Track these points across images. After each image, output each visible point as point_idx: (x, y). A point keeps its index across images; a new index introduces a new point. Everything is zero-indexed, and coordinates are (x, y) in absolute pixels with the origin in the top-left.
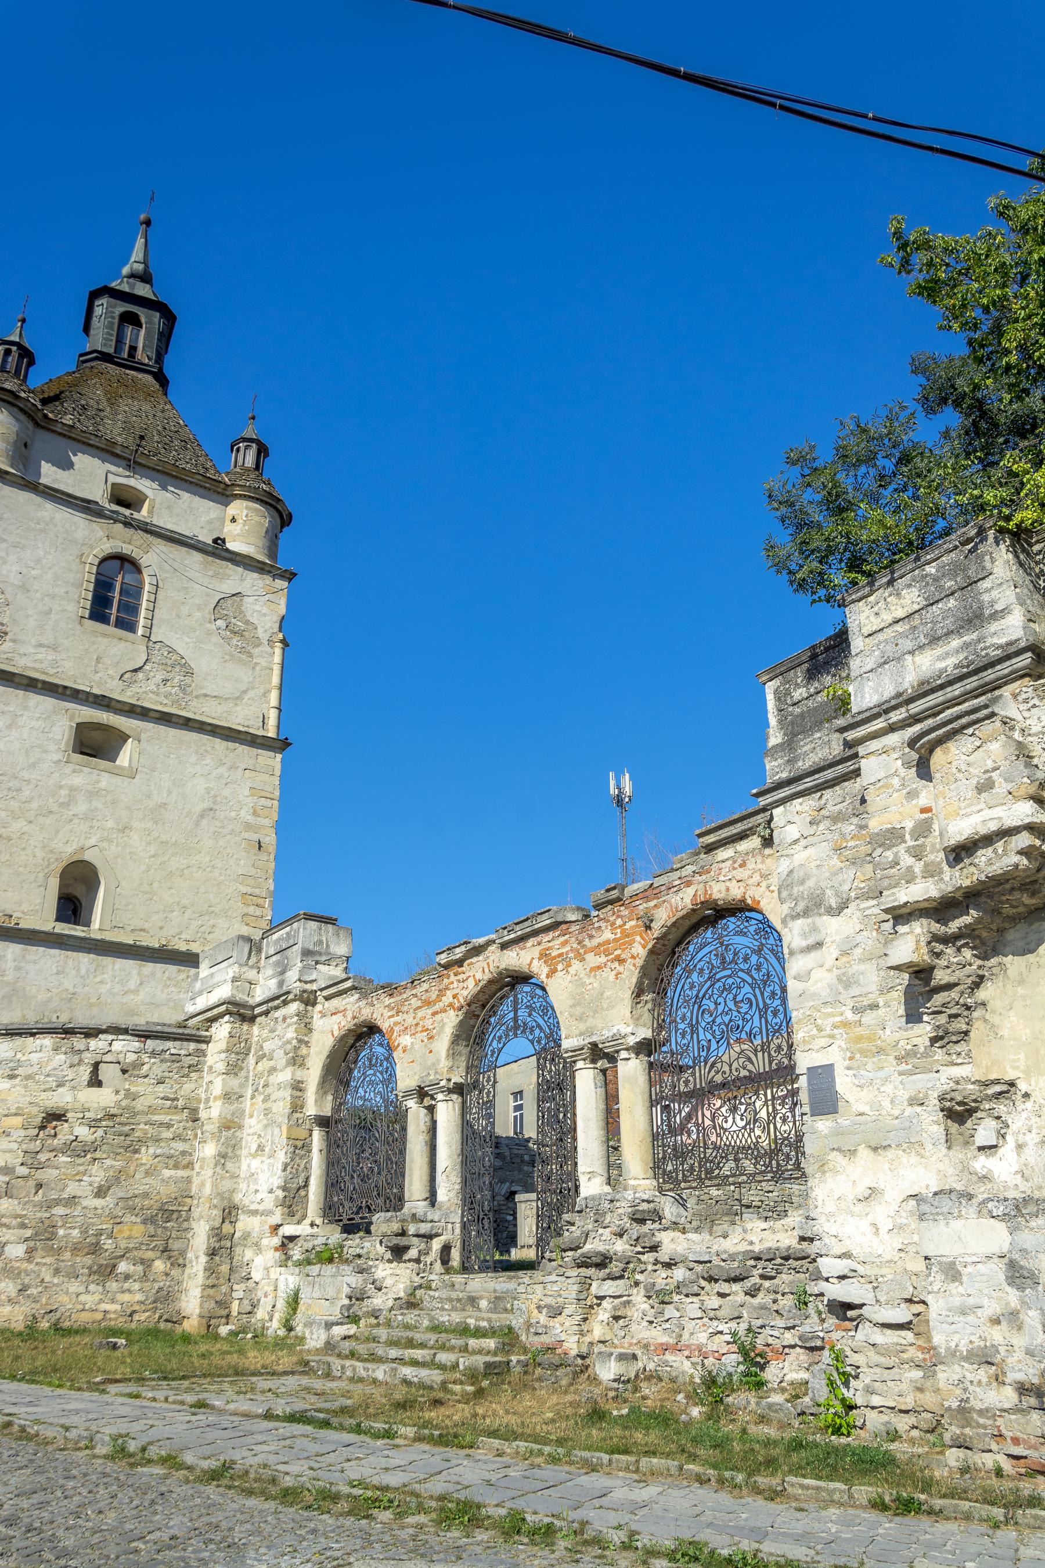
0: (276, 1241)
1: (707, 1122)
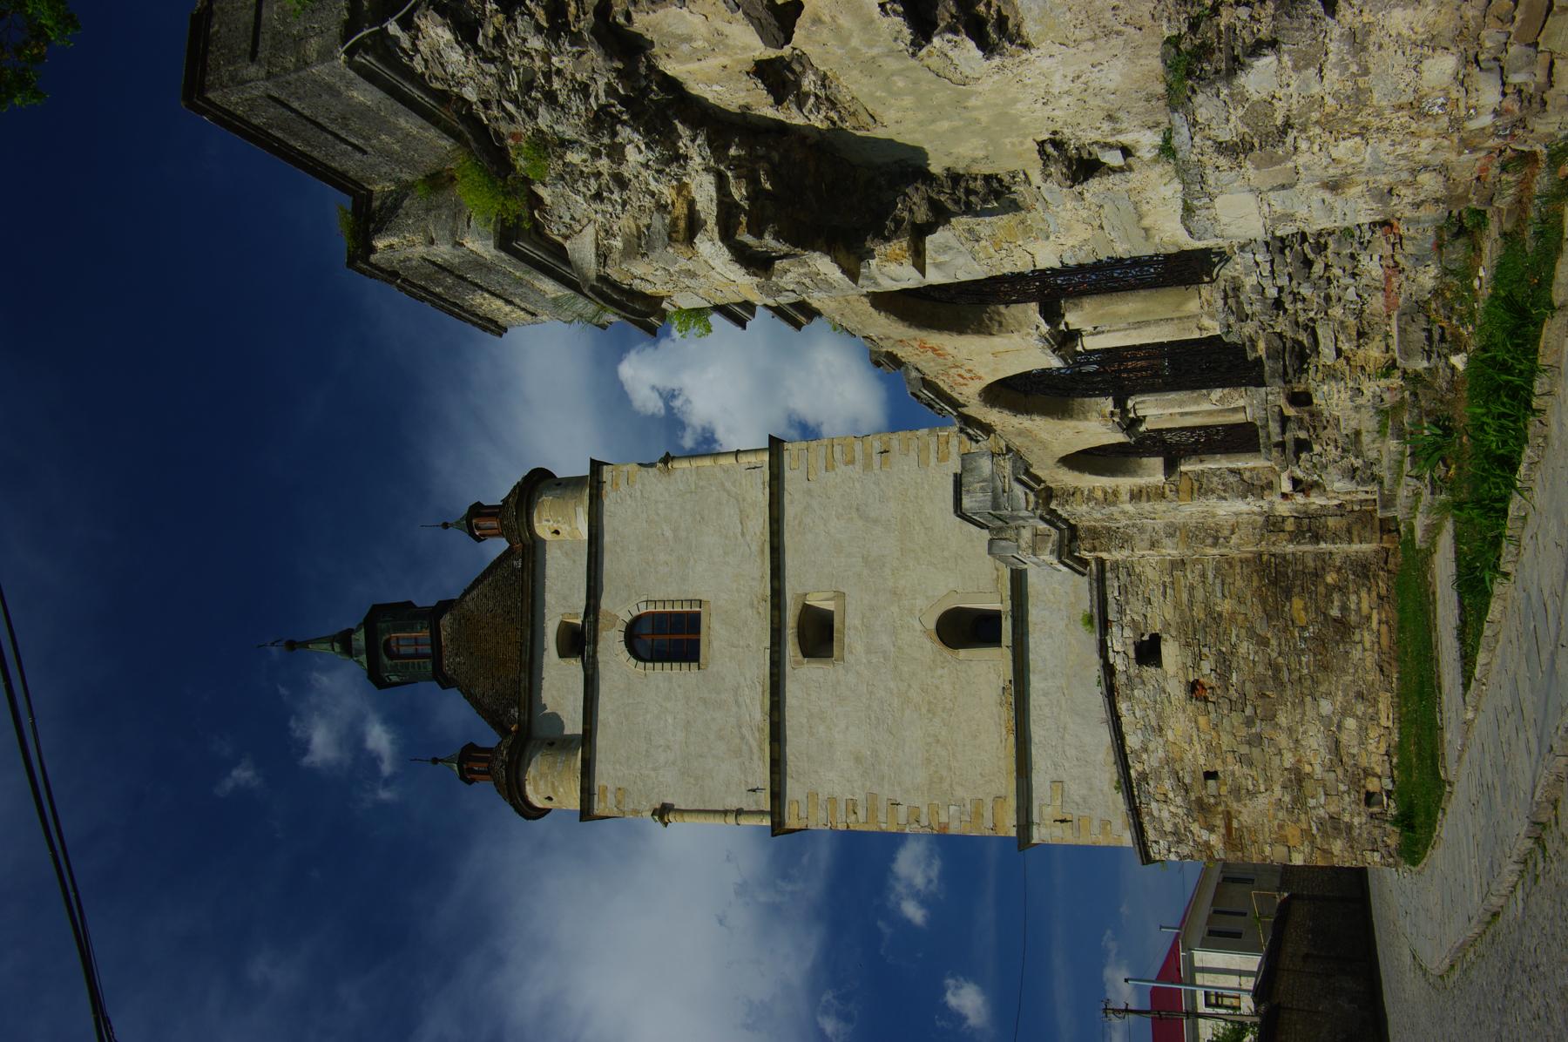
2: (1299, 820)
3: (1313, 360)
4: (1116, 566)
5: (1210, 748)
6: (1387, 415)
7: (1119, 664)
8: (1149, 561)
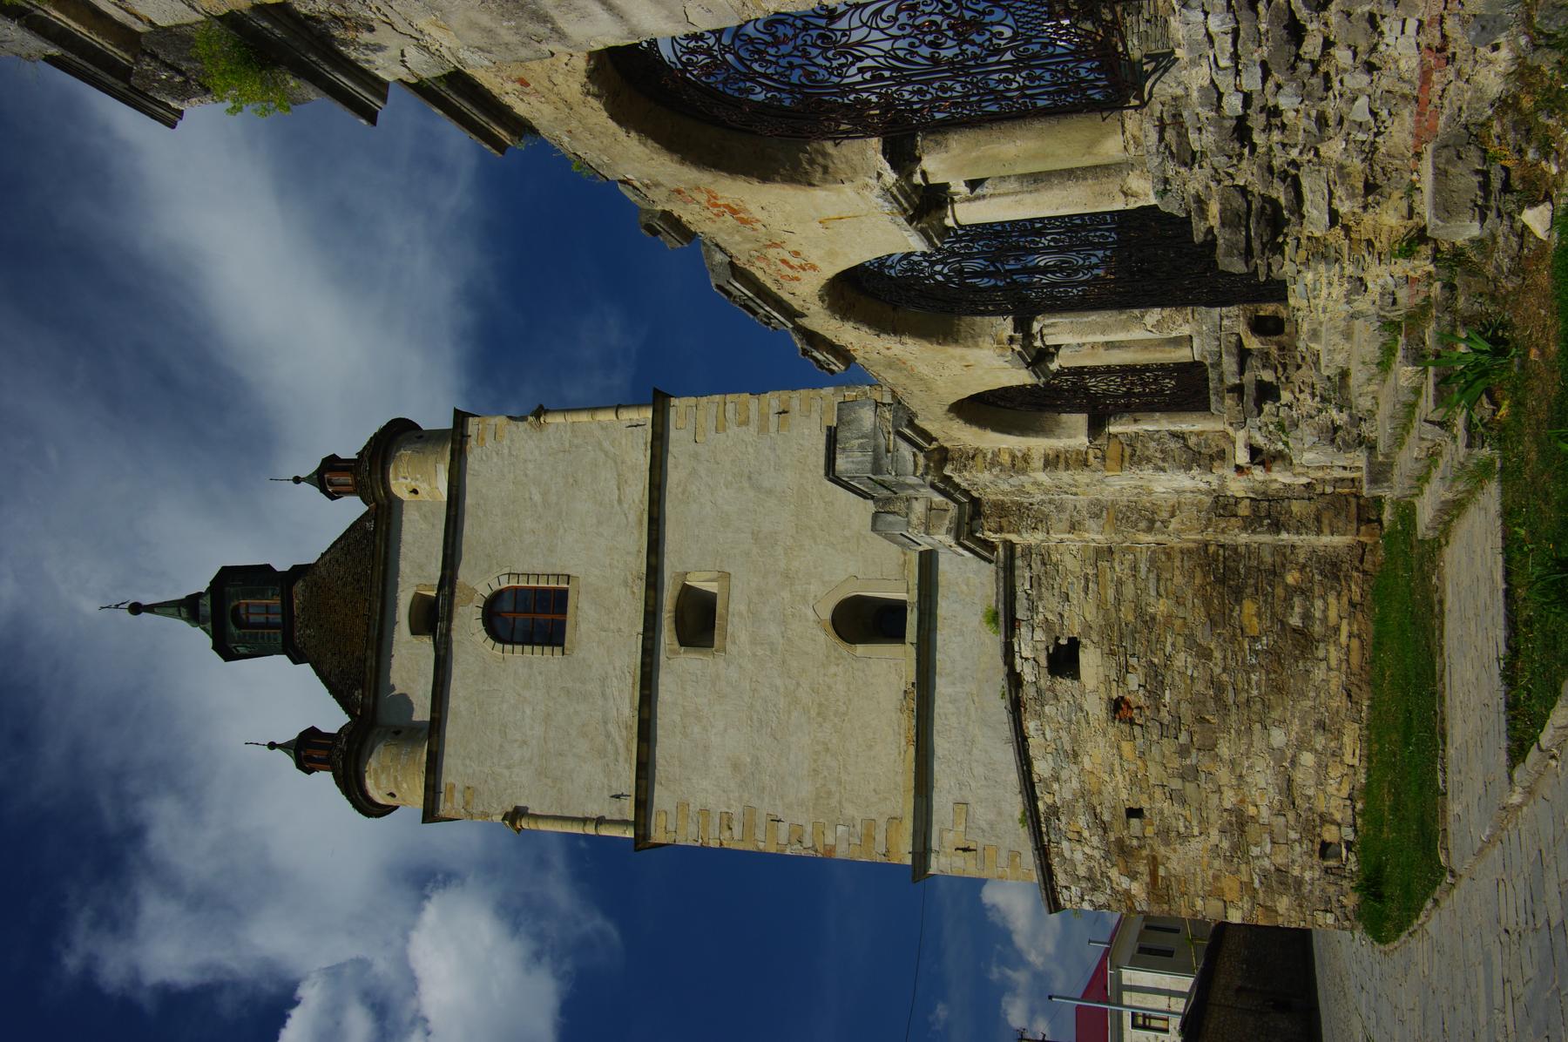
1: (1008, 56)
2: (1238, 870)
3: (1292, 230)
4: (1028, 551)
5: (1135, 781)
6: (1399, 329)
7: (1028, 672)
8: (1068, 547)
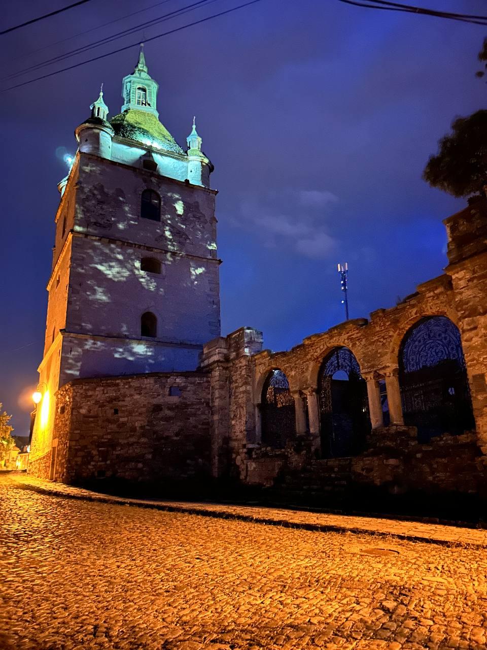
0: (245, 450)
